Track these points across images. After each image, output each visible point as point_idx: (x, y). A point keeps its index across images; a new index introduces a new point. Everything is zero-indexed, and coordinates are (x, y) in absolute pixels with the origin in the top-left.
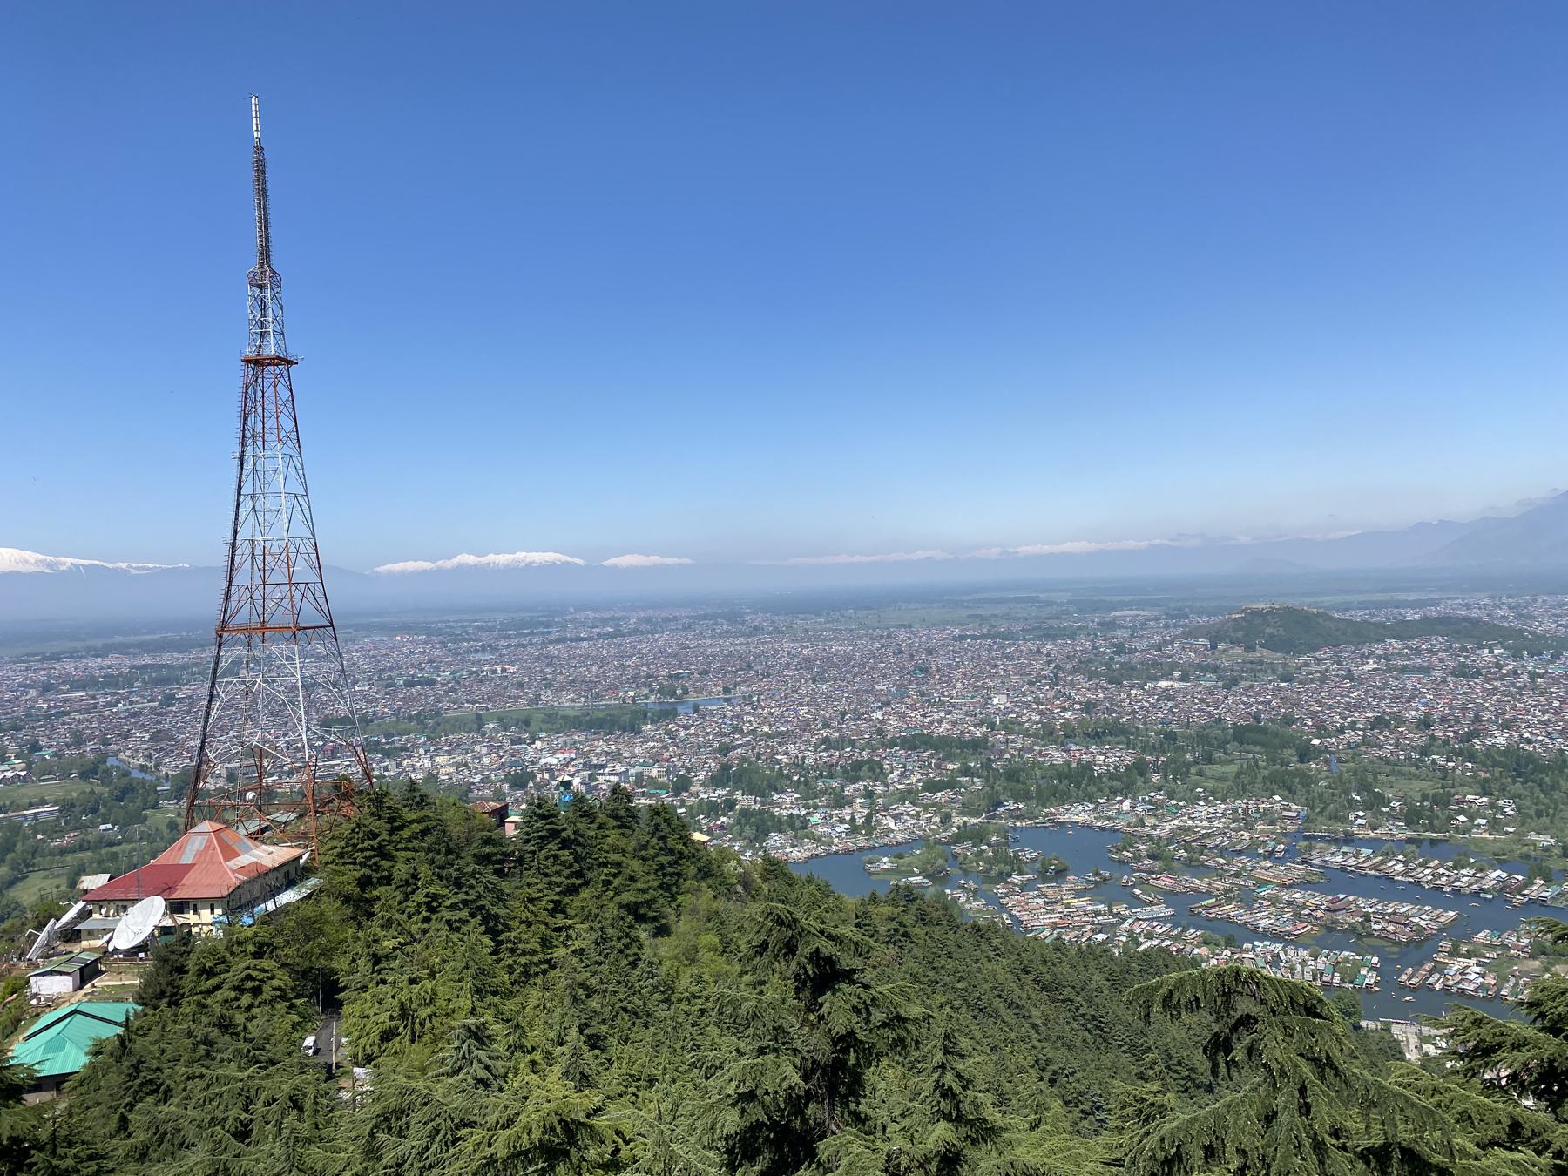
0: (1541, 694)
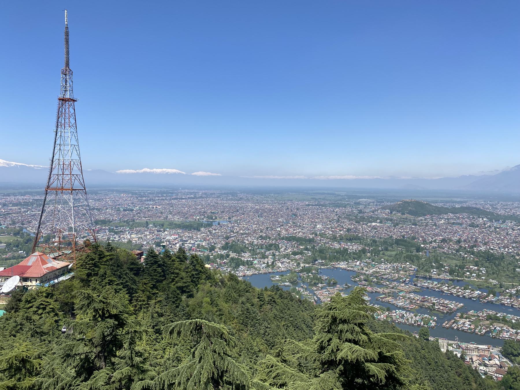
0: (498, 234)
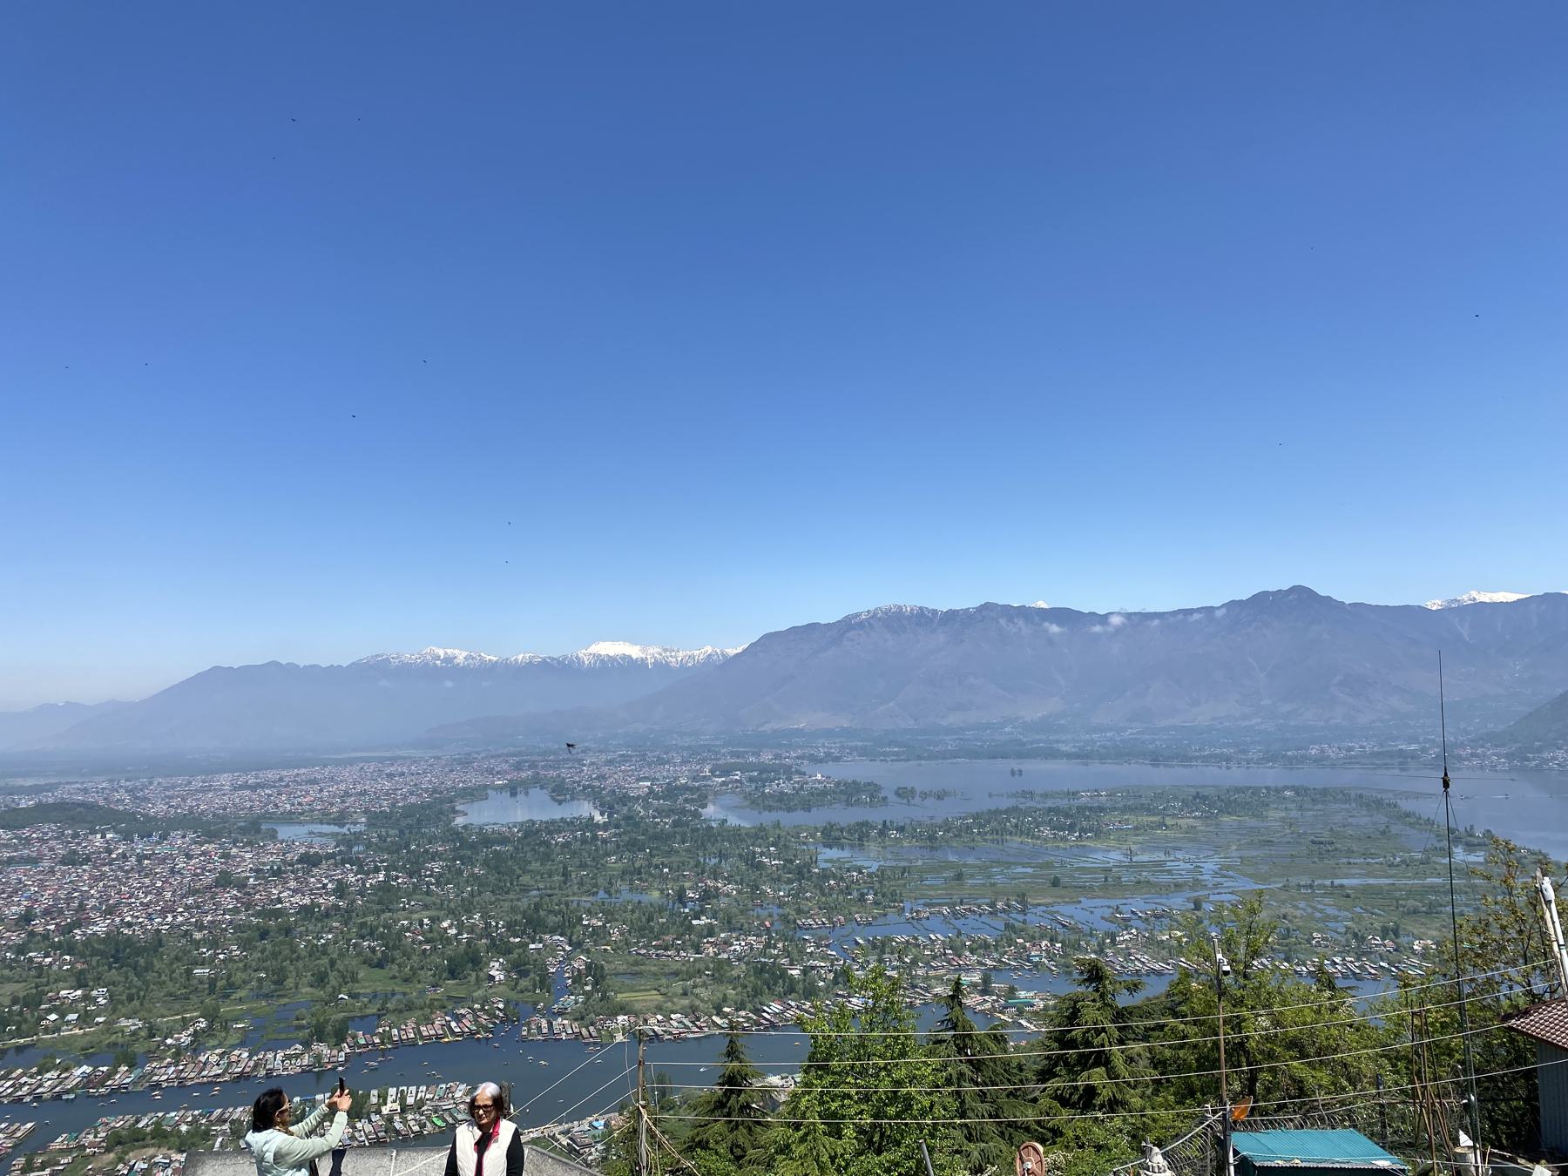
0: (146, 876)
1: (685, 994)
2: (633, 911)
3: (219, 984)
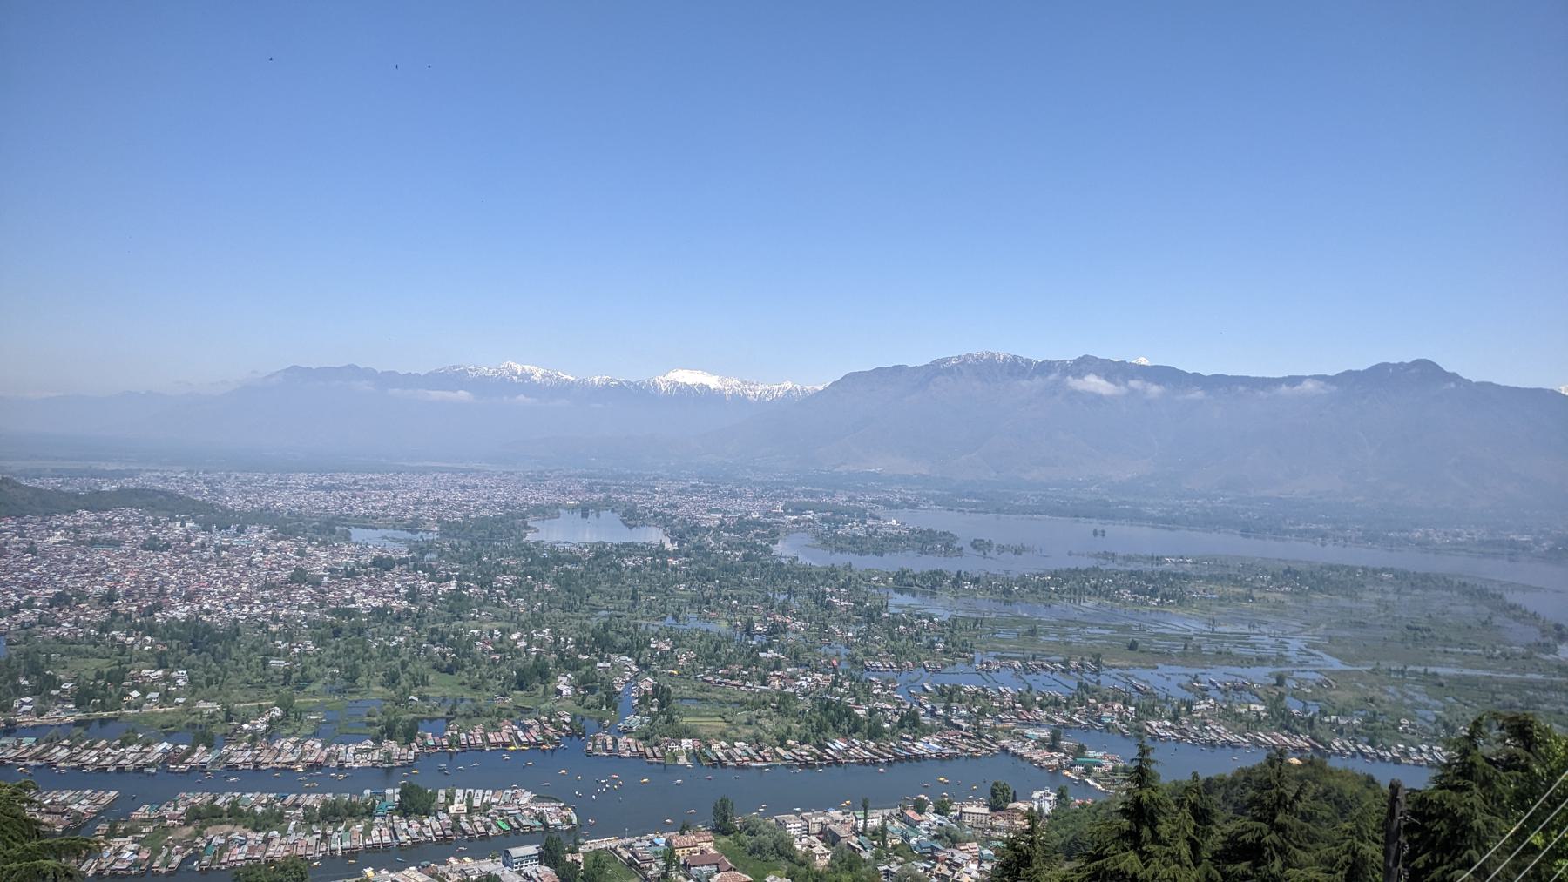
0: (224, 566)
1: (749, 723)
2: (700, 639)
3: (294, 676)
